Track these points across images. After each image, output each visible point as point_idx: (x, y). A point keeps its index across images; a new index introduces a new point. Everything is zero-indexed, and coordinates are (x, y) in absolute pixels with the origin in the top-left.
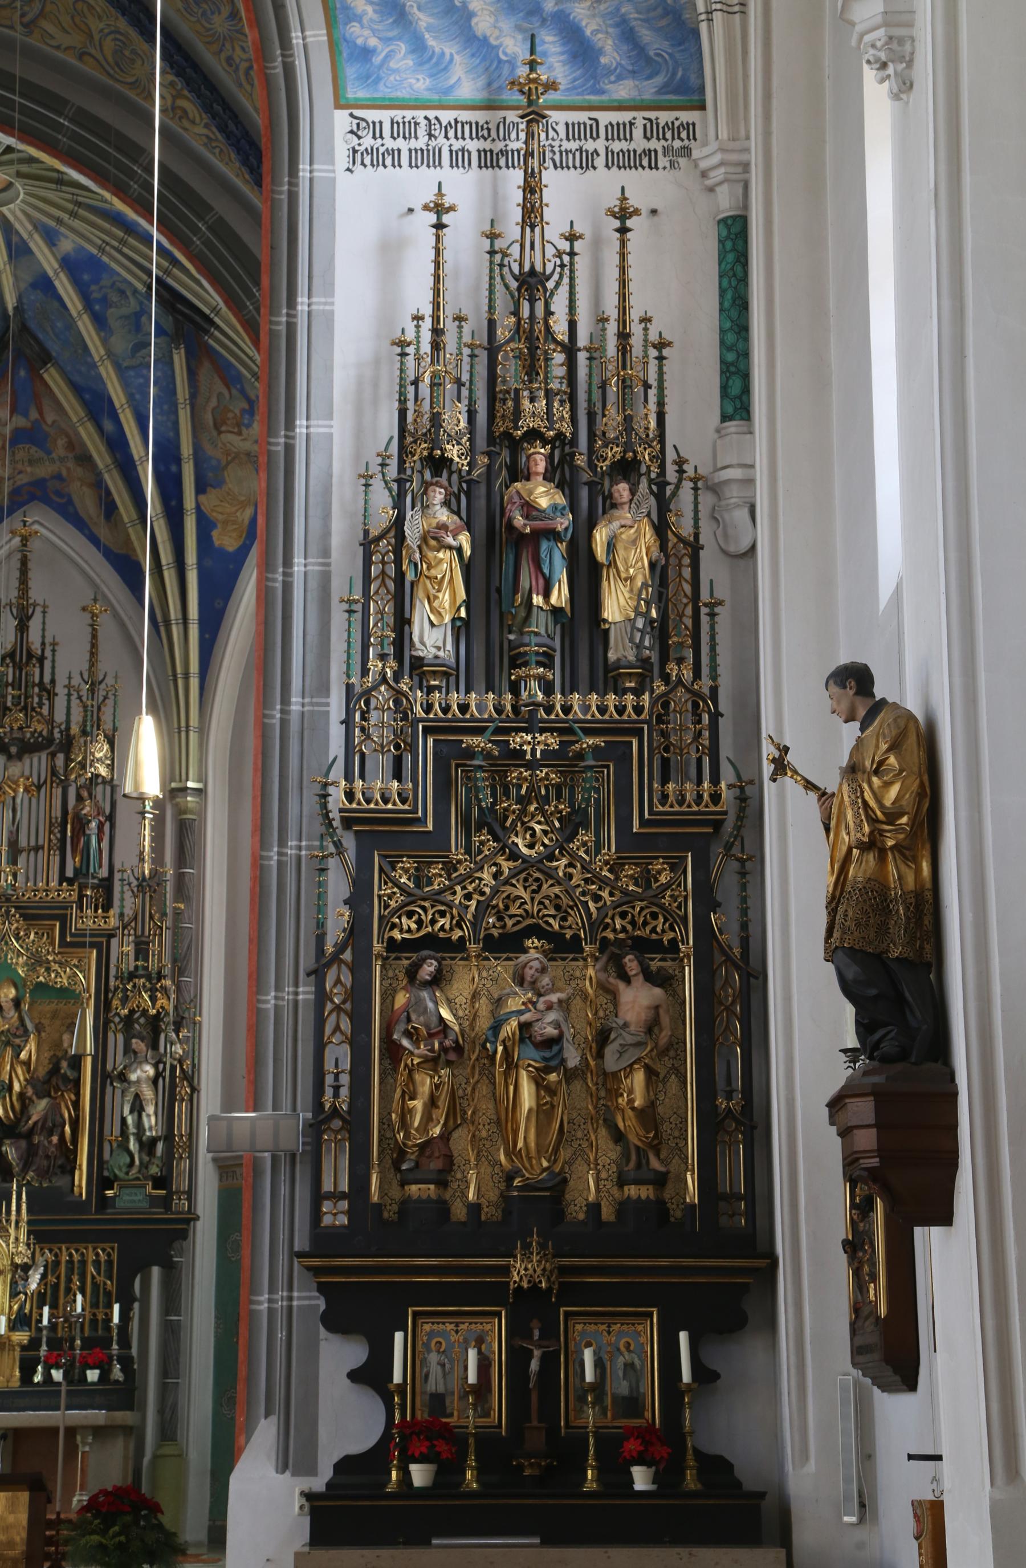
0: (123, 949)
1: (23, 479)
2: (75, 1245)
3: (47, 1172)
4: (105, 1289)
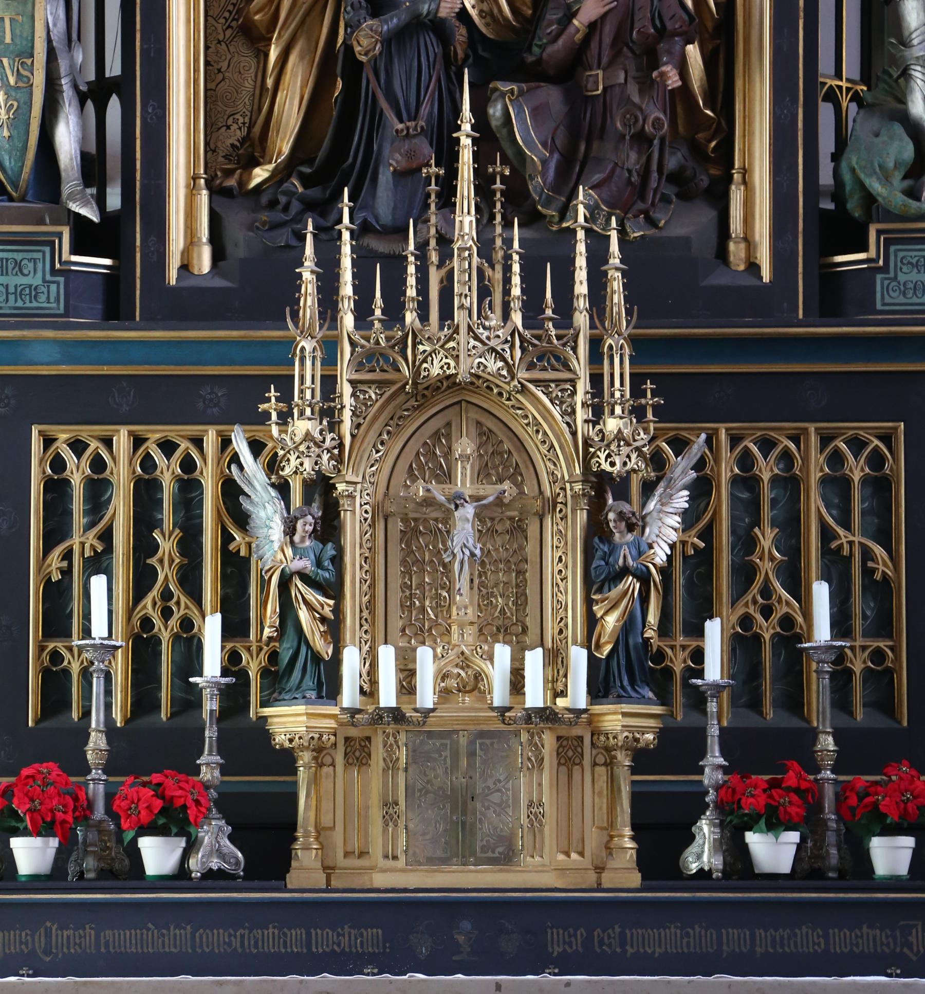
2: (762, 428)
3: (641, 191)
4: (868, 573)
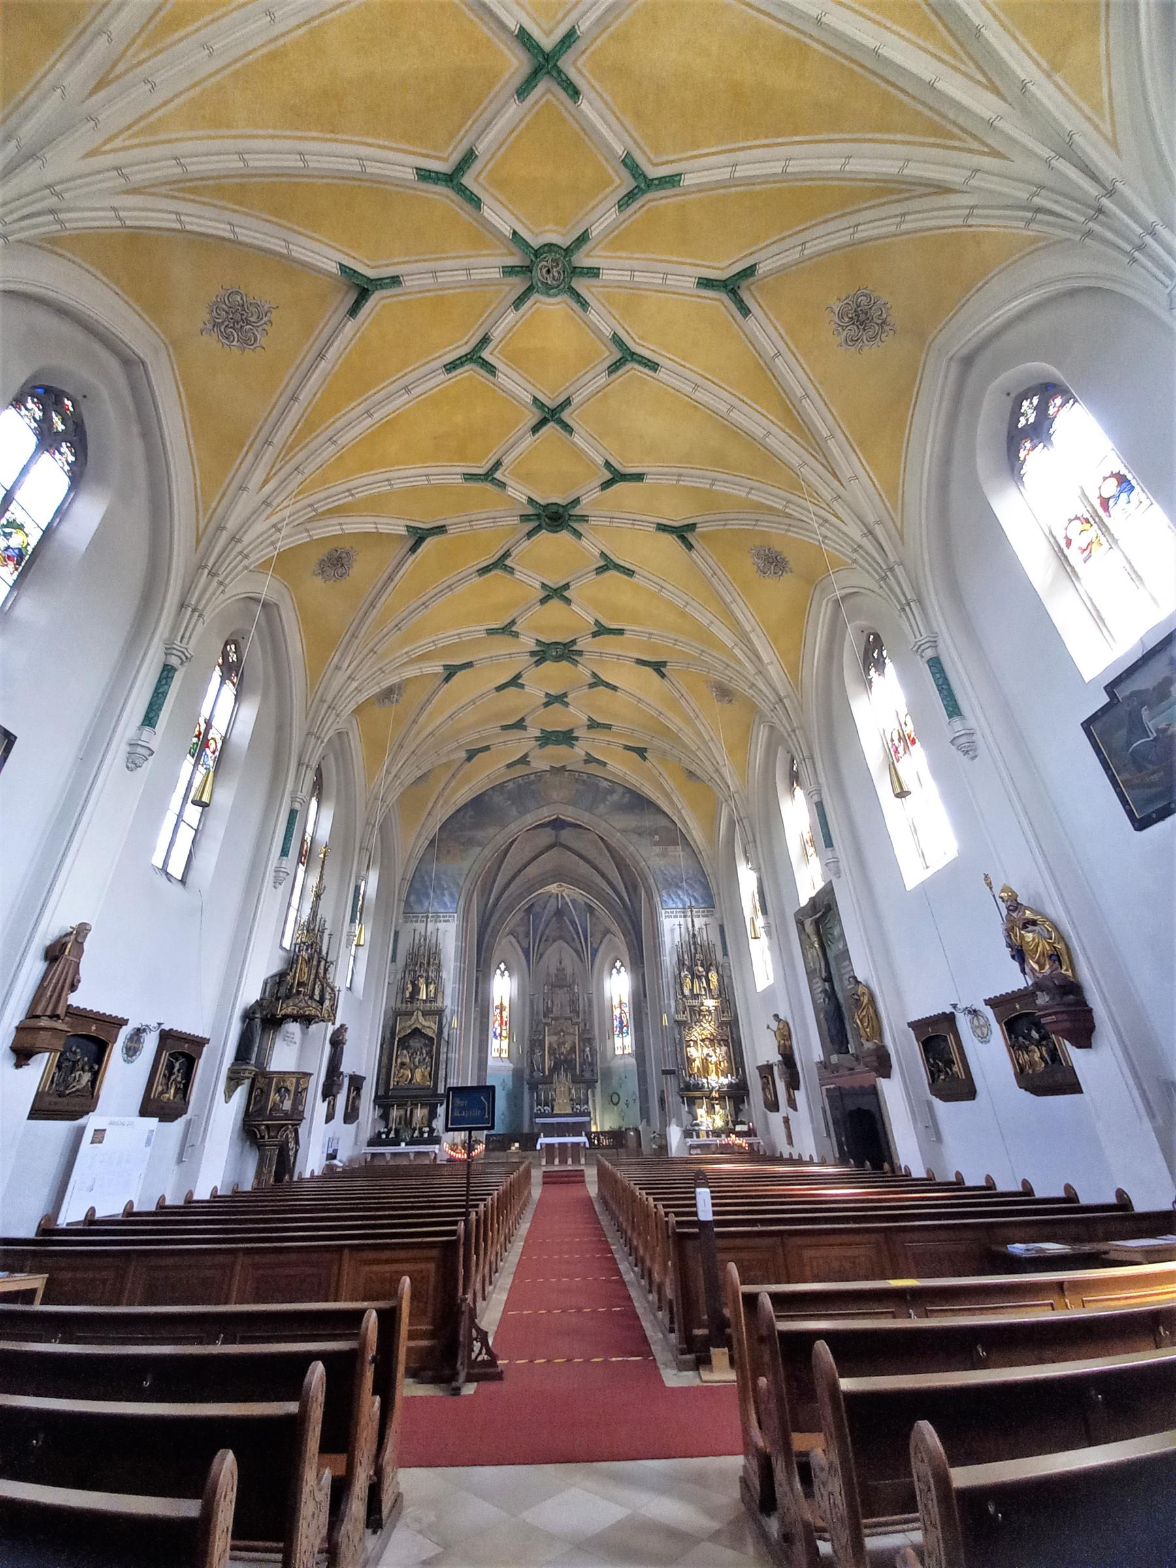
0: (582, 1025)
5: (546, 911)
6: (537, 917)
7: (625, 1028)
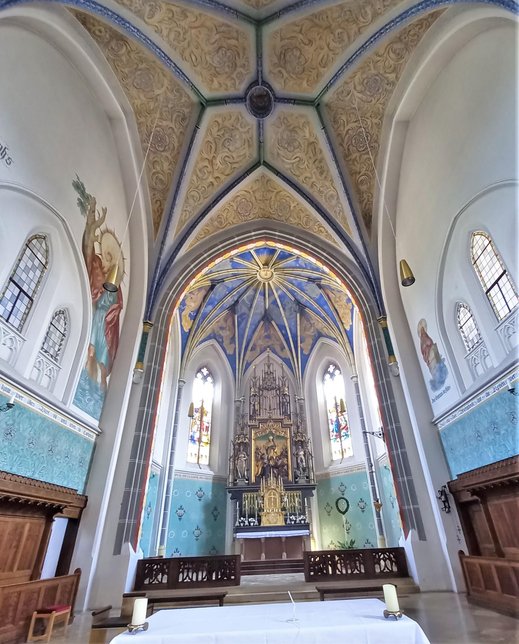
1: (266, 346)
5: (253, 310)
6: (243, 318)
7: (344, 431)
